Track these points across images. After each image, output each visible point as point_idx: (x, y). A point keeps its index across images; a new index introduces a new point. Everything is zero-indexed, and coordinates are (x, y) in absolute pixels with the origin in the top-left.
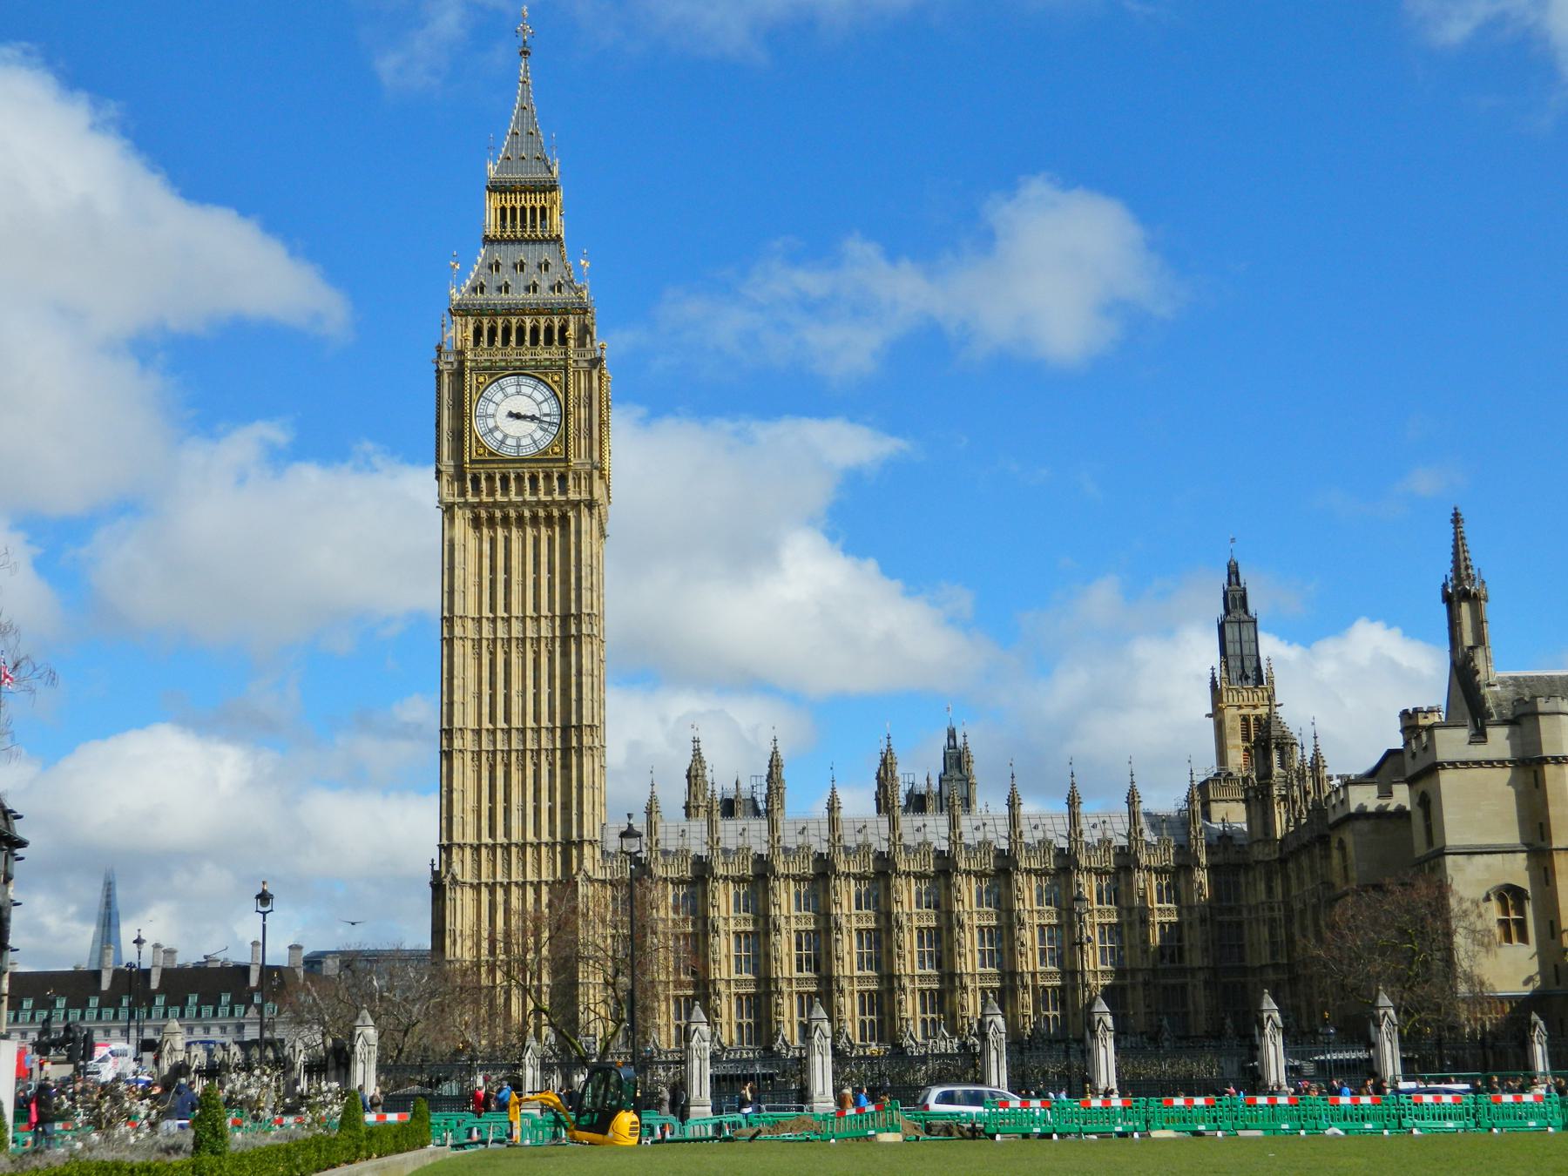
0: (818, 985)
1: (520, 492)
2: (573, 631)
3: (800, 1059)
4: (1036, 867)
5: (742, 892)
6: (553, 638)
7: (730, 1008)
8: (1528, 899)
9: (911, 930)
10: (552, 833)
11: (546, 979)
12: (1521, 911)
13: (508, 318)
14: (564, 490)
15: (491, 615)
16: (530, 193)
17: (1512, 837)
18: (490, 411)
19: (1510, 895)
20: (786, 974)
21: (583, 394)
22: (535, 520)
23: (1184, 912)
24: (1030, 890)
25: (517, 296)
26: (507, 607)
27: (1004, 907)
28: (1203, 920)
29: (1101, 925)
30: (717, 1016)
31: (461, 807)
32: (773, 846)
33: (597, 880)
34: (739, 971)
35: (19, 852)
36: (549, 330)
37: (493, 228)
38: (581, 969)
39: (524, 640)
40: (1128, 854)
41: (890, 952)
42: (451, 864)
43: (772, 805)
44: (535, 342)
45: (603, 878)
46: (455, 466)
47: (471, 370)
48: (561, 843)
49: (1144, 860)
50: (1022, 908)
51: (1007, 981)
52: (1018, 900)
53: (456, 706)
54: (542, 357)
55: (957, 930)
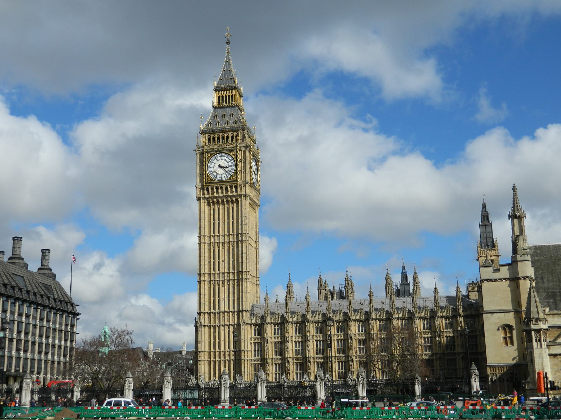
1: (222, 193)
2: (240, 239)
3: (314, 385)
4: (401, 317)
6: (234, 242)
8: (514, 329)
9: (356, 340)
10: (234, 308)
11: (232, 358)
12: (511, 334)
14: (236, 191)
15: (214, 235)
17: (509, 307)
18: (212, 166)
19: (507, 328)
20: (312, 355)
21: (243, 158)
22: (228, 202)
23: (455, 332)
25: (222, 126)
26: (219, 232)
28: (461, 335)
29: (425, 338)
30: (288, 370)
31: (204, 300)
34: (296, 355)
35: (78, 317)
36: (232, 137)
38: (242, 354)
39: (224, 243)
40: (434, 312)
41: (348, 347)
45: (251, 323)
49: (440, 314)
53: (202, 266)
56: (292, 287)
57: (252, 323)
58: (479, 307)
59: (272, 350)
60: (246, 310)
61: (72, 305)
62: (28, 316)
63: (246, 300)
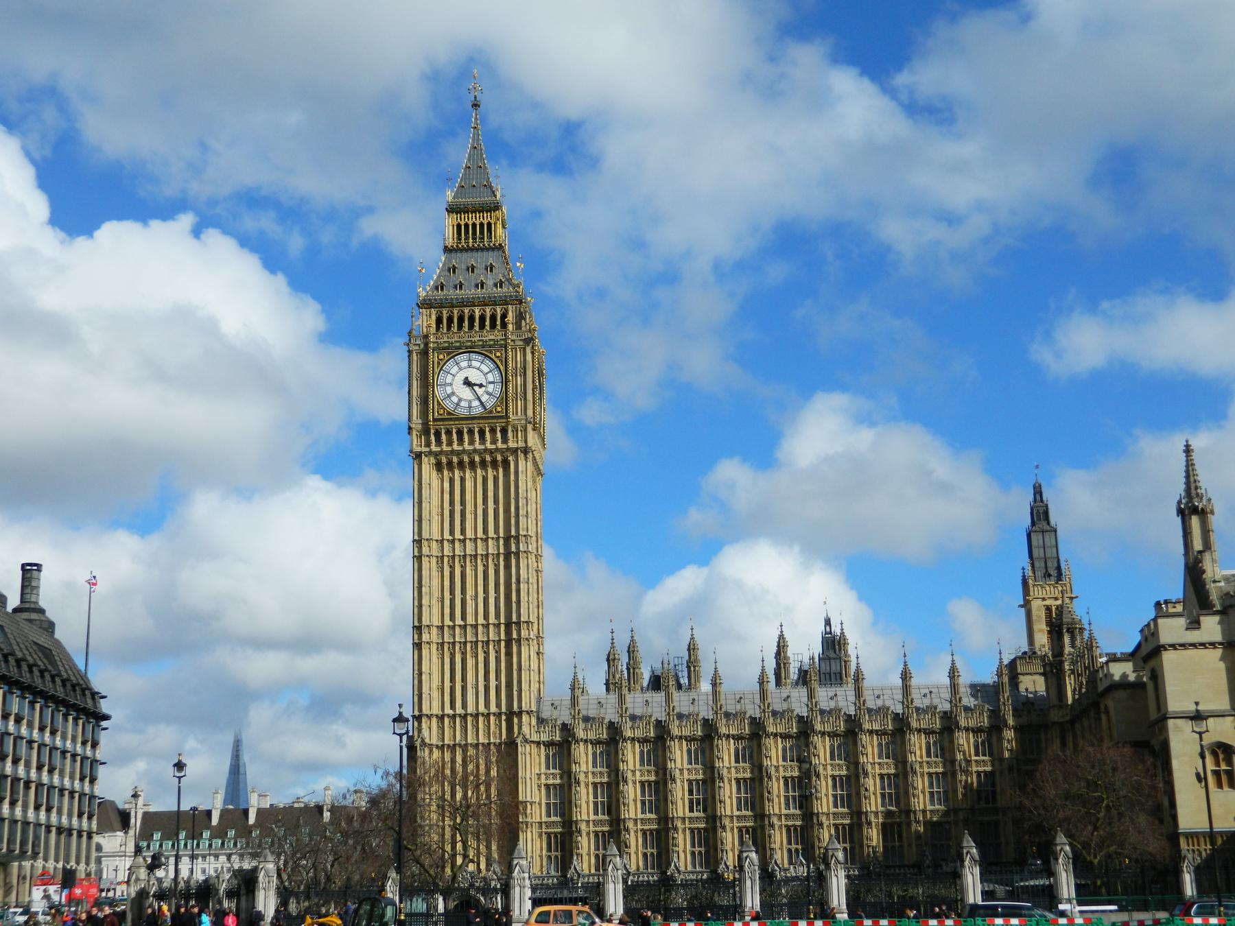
0: (707, 823)
1: (472, 442)
2: (513, 548)
4: (877, 728)
5: (645, 750)
6: (498, 554)
7: (637, 841)
9: (778, 779)
10: (498, 705)
13: (462, 309)
14: (505, 440)
15: (451, 538)
18: (448, 381)
20: (680, 814)
21: (519, 366)
22: (483, 464)
24: (873, 747)
25: (469, 292)
26: (463, 532)
27: (852, 760)
30: (626, 847)
31: (428, 686)
32: (669, 714)
33: (533, 742)
36: (493, 318)
39: (476, 556)
41: (762, 796)
43: (668, 682)
44: (482, 326)
45: (538, 740)
46: (422, 424)
47: (433, 350)
48: (505, 713)
50: (866, 761)
51: (855, 820)
53: (424, 608)
54: (487, 338)
55: (814, 778)
57: (542, 739)
58: (1050, 707)
59: (588, 803)
61: (94, 695)
62: (18, 720)
63: (528, 688)
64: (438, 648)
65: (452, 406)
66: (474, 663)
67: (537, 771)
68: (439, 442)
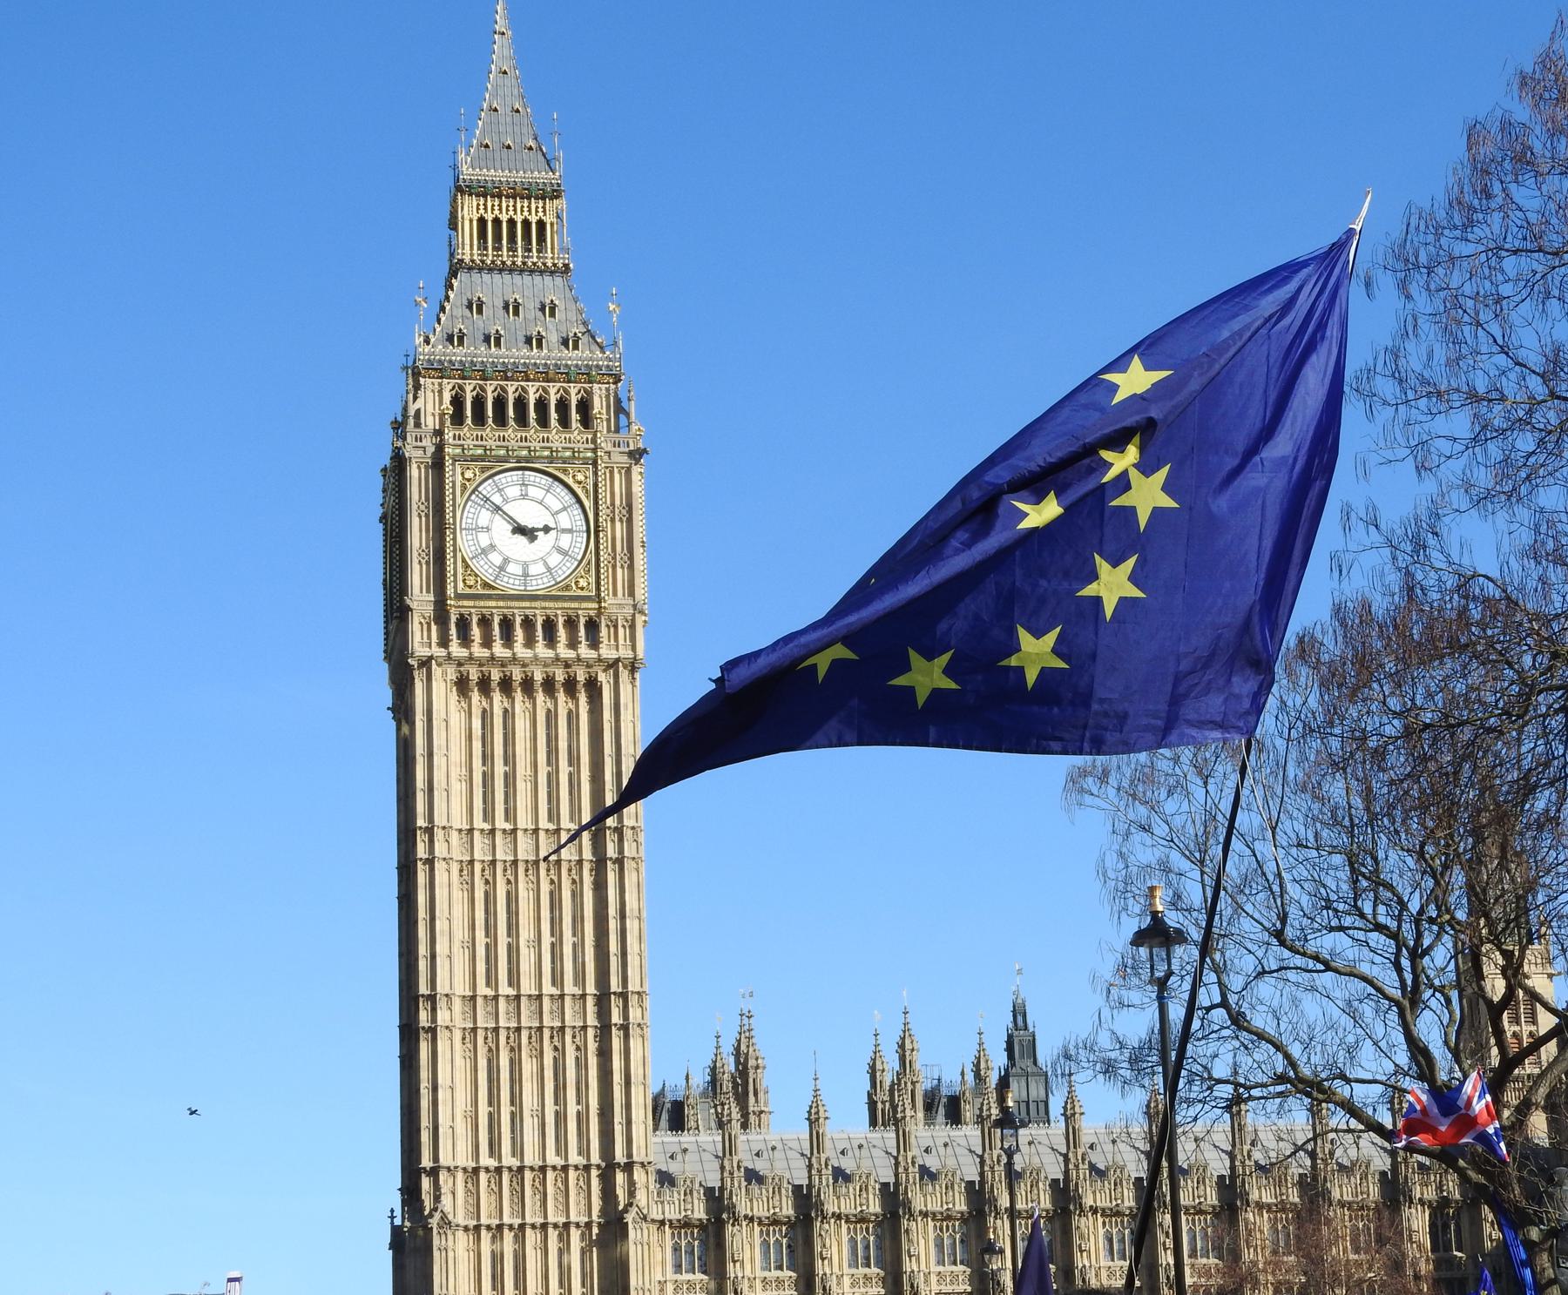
4: (1269, 1201)
5: (859, 1238)
6: (580, 862)
10: (584, 1150)
14: (594, 643)
15: (487, 826)
16: (522, 198)
25: (514, 353)
33: (653, 1221)
37: (467, 247)
42: (439, 1196)
45: (660, 1217)
46: (436, 603)
48: (598, 1167)
52: (823, 1259)
56: (764, 1068)
57: (668, 1216)
60: (645, 1161)
64: (464, 1039)
65: (490, 571)
66: (535, 1070)
67: (659, 1277)
68: (465, 640)
